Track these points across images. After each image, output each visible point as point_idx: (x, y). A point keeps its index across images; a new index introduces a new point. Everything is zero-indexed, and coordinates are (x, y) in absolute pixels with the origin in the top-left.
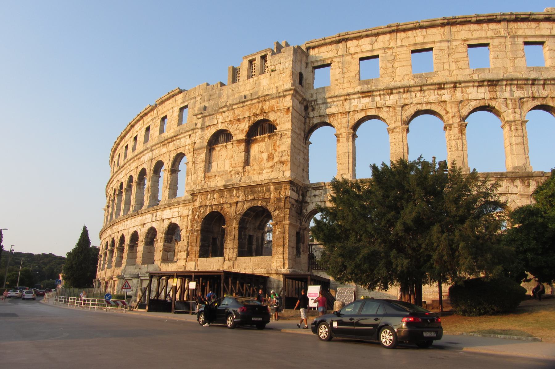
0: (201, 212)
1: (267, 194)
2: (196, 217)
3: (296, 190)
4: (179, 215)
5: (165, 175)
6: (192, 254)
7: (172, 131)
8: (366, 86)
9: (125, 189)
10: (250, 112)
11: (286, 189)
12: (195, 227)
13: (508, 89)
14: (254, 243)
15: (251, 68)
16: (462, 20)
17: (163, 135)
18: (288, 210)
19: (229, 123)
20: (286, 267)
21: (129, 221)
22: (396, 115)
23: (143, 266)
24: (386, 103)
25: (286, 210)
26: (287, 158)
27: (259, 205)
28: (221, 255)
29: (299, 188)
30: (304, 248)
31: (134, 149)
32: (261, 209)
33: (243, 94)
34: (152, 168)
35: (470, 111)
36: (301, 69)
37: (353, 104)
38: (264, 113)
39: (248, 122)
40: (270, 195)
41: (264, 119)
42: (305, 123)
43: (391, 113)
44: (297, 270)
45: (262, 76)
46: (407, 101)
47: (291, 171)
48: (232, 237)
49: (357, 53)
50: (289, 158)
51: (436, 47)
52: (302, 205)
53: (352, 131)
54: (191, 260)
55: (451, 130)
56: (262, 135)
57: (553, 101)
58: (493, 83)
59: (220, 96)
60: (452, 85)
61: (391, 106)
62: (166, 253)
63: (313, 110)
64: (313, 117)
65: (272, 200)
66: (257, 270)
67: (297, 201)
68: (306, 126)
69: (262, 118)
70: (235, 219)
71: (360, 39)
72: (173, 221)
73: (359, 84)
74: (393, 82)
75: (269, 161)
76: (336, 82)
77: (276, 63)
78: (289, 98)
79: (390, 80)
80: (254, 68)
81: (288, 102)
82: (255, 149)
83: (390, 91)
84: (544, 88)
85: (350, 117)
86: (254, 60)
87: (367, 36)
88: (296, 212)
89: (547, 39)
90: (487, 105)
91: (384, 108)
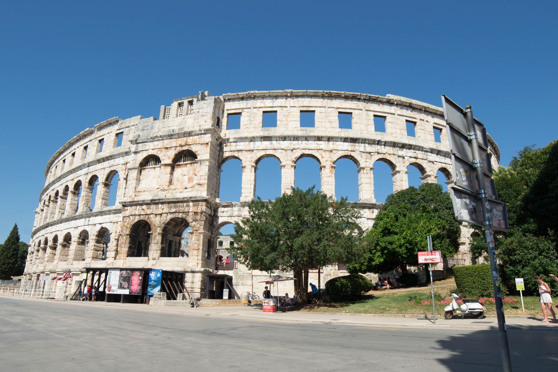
0: (131, 220)
1: (187, 208)
2: (126, 224)
3: (210, 207)
4: (110, 221)
5: (100, 189)
6: (121, 253)
7: (108, 151)
8: (267, 132)
9: (61, 197)
10: (177, 143)
11: (202, 205)
12: (125, 232)
13: (363, 145)
14: (173, 247)
15: (180, 109)
16: (336, 94)
18: (203, 222)
19: (158, 150)
20: (200, 265)
21: (63, 224)
22: (287, 155)
23: (74, 262)
24: (280, 146)
25: (201, 222)
26: (205, 181)
27: (180, 217)
28: (146, 255)
29: (212, 205)
30: (213, 252)
31: (71, 164)
32: (181, 220)
33: (172, 128)
34: (88, 180)
35: (338, 157)
36: (219, 114)
37: (256, 145)
38: (188, 145)
39: (175, 151)
40: (189, 209)
41: (187, 149)
42: (219, 155)
44: (207, 269)
45: (189, 116)
46: (296, 147)
47: (207, 192)
48: (156, 241)
49: (262, 107)
50: (206, 182)
51: (317, 110)
52: (213, 219)
53: (254, 164)
54: (120, 259)
55: (324, 170)
56: (185, 161)
57: (390, 156)
58: (354, 140)
59: (152, 128)
60: (327, 139)
61: (283, 149)
62: (96, 252)
63: (226, 146)
64: (226, 151)
65: (190, 214)
66: (176, 268)
67: (210, 215)
68: (220, 158)
69: (186, 149)
70: (159, 227)
71: (265, 98)
72: (104, 226)
73: (262, 130)
74: (287, 131)
75: (189, 183)
76: (245, 127)
78: (209, 135)
79: (284, 130)
80: (182, 109)
81: (208, 138)
82: (178, 171)
83: (284, 138)
84: (385, 147)
85: (253, 154)
86: (183, 103)
87: (270, 96)
88: (209, 224)
89: (388, 115)
90: (349, 155)
91: (279, 150)
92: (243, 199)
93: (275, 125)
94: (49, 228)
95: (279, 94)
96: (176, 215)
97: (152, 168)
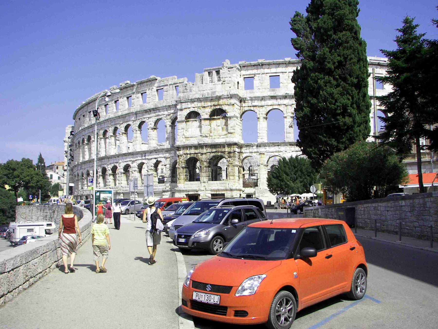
8: (273, 92)
17: (145, 104)
34: (137, 125)
38: (219, 105)
42: (240, 109)
43: (285, 108)
49: (268, 73)
53: (265, 116)
59: (191, 91)
63: (245, 102)
64: (245, 107)
72: (159, 159)
73: (270, 91)
77: (225, 77)
82: (214, 123)
87: (274, 64)
92: (260, 141)
93: (278, 86)
94: (105, 160)
95: (280, 63)
96: (217, 154)
97: (194, 121)
